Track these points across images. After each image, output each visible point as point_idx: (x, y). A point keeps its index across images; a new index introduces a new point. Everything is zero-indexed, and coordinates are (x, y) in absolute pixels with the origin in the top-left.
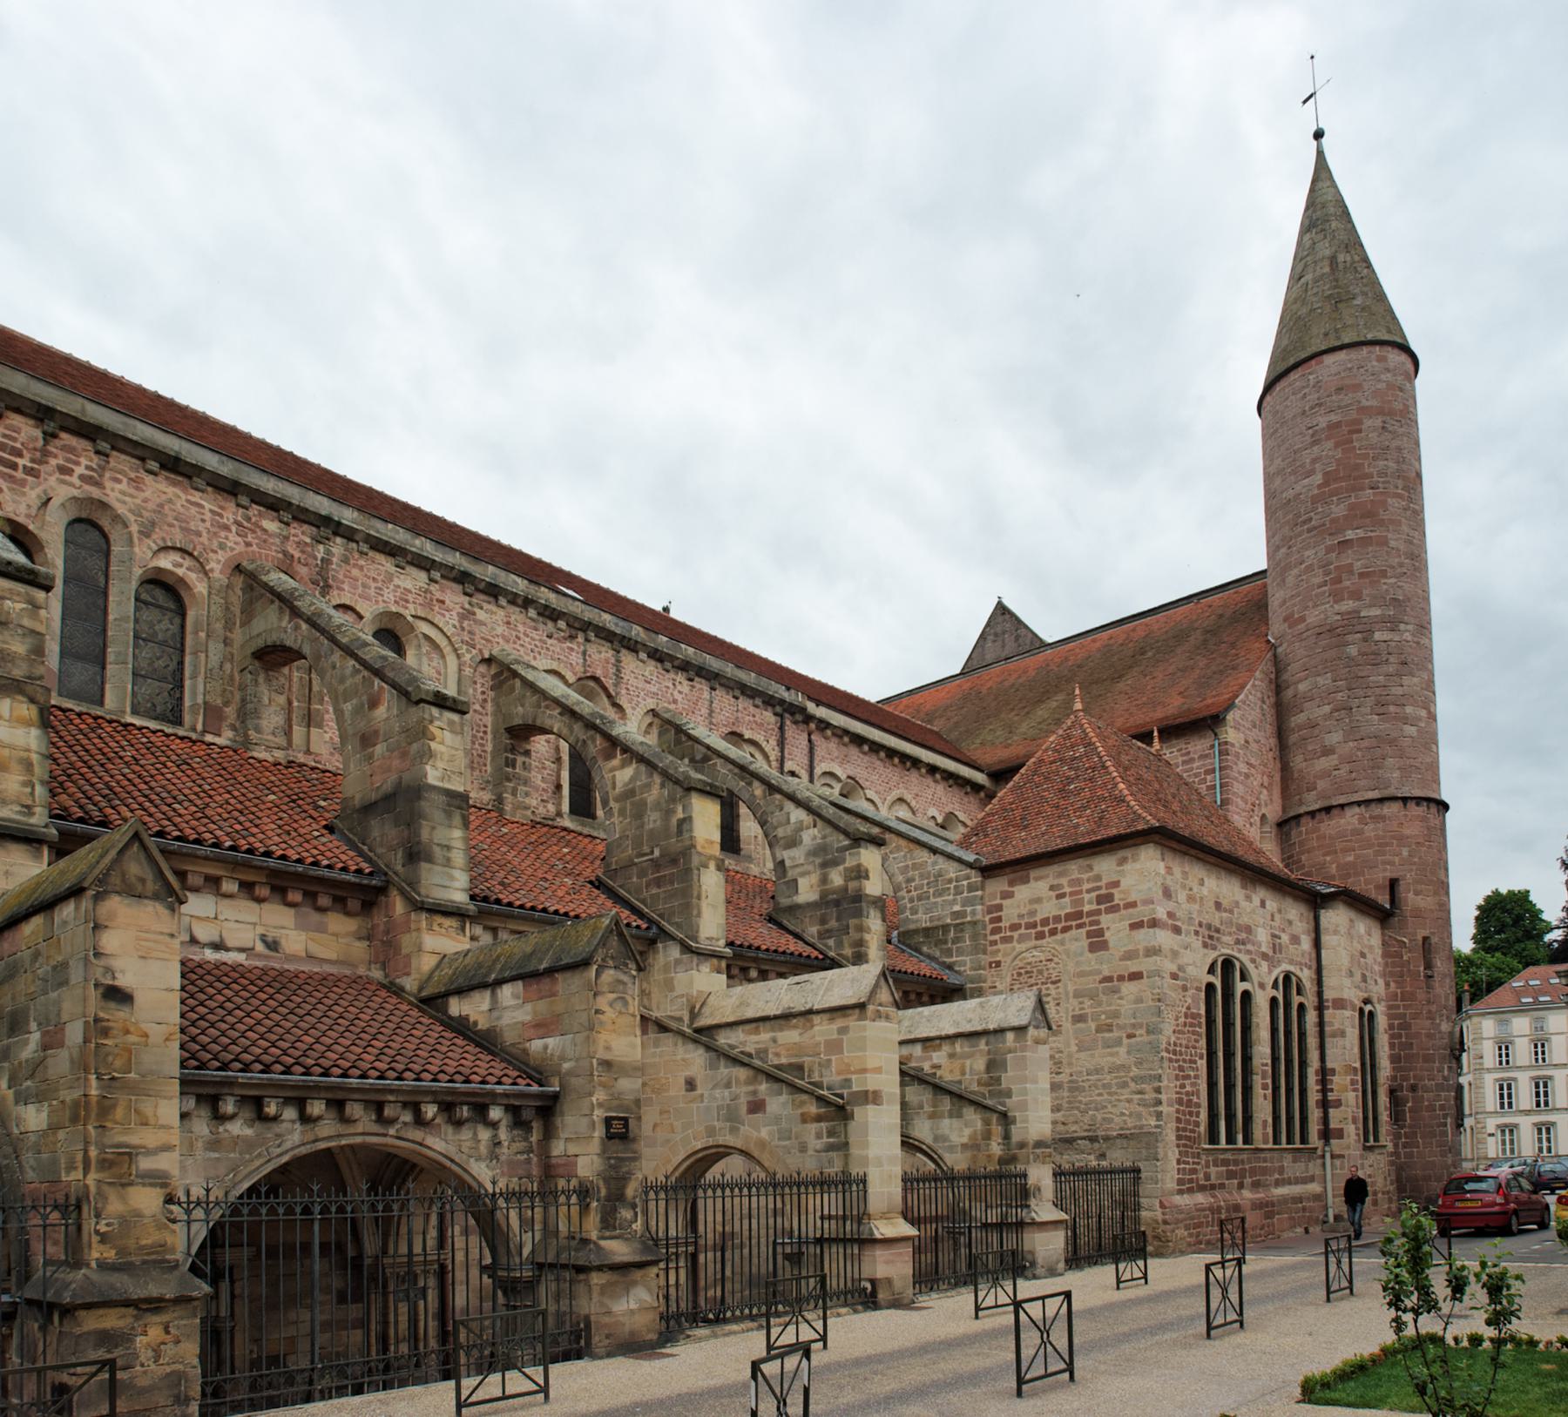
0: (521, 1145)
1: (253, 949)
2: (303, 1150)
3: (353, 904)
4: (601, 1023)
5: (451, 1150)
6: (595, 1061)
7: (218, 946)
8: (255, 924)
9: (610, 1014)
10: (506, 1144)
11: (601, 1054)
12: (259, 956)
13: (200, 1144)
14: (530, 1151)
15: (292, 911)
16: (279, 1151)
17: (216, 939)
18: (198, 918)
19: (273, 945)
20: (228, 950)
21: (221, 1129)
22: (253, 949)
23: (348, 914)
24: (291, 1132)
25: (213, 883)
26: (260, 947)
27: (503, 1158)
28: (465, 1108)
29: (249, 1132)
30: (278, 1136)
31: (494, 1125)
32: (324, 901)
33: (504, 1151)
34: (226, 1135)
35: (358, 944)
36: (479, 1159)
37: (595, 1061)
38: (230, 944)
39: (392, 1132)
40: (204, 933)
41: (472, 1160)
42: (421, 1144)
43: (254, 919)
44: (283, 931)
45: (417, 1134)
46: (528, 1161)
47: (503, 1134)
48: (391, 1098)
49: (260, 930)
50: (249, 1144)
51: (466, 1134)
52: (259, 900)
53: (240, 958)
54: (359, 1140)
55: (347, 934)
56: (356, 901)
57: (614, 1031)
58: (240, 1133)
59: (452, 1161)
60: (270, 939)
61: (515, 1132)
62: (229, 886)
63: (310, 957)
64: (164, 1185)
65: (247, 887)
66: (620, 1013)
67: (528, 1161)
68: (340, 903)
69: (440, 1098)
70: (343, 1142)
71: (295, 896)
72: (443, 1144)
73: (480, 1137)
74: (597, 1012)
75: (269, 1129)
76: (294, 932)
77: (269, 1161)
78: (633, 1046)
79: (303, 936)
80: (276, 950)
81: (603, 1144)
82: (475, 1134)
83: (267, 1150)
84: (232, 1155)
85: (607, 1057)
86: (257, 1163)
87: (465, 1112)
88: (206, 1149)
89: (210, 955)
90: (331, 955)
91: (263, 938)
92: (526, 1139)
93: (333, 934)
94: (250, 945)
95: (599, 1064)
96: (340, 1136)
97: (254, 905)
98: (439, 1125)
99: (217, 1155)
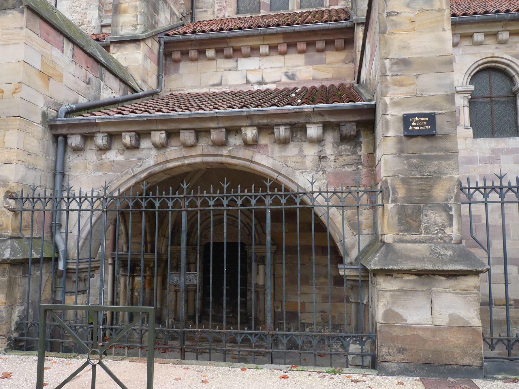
0: (350, 158)
1: (281, 81)
2: (157, 169)
3: (339, 43)
4: (395, 24)
5: (278, 165)
6: (387, 62)
7: (260, 83)
8: (281, 67)
9: (407, 14)
10: (332, 158)
11: (395, 54)
12: (284, 84)
13: (91, 167)
14: (359, 162)
15: (303, 56)
16: (140, 169)
17: (260, 79)
18: (250, 70)
19: (291, 77)
20: (266, 84)
21: (104, 156)
22: (281, 81)
23: (338, 50)
24: (148, 157)
25: (255, 50)
26: (284, 79)
27: (328, 170)
28: (282, 129)
29: (121, 157)
30: (140, 159)
31: (319, 141)
32: (320, 45)
33: (331, 165)
34: (106, 160)
35: (345, 66)
36: (304, 171)
37: (387, 62)
38: (267, 80)
39: (225, 152)
40: (253, 78)
41: (297, 172)
42: (251, 162)
43: (281, 65)
44: (298, 68)
45: (246, 153)
46: (357, 172)
47: (329, 150)
48: (212, 125)
49: (284, 70)
50: (120, 166)
51: (292, 150)
52: (283, 54)
53: (272, 87)
54: (198, 160)
55: (338, 62)
56: (340, 41)
57: (413, 29)
58: (116, 159)
59: (280, 174)
60: (290, 74)
61: (343, 147)
62: (264, 49)
63: (314, 79)
64: (5, 186)
65: (273, 48)
66: (422, 11)
67: (357, 172)
68: (329, 43)
69: (257, 121)
70: (187, 162)
71: (302, 46)
72: (271, 160)
73: (305, 153)
74: (389, 14)
75: (134, 155)
76: (304, 67)
77: (133, 176)
78: (442, 40)
79: (310, 68)
80: (294, 80)
81: (399, 141)
82: (301, 151)
83: (132, 170)
84: (110, 173)
85: (405, 55)
86: (125, 178)
87: (282, 132)
88: (94, 170)
89: (256, 88)
90: (329, 76)
91: (286, 75)
92: (354, 153)
93: (330, 63)
94: (279, 79)
95: (393, 64)
96: (184, 158)
97: (281, 58)
98: (266, 146)
99: (100, 173)
